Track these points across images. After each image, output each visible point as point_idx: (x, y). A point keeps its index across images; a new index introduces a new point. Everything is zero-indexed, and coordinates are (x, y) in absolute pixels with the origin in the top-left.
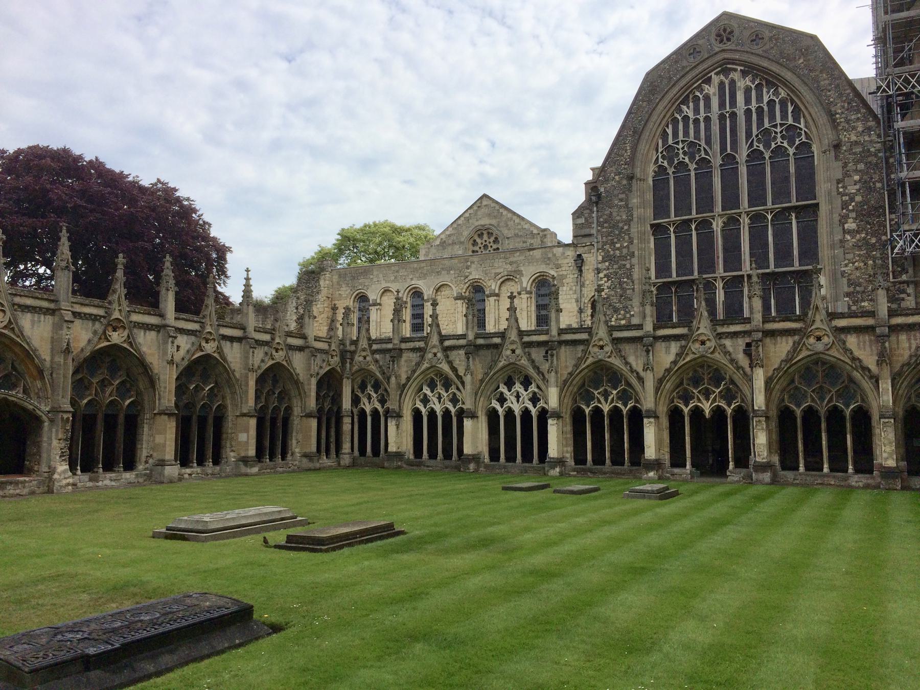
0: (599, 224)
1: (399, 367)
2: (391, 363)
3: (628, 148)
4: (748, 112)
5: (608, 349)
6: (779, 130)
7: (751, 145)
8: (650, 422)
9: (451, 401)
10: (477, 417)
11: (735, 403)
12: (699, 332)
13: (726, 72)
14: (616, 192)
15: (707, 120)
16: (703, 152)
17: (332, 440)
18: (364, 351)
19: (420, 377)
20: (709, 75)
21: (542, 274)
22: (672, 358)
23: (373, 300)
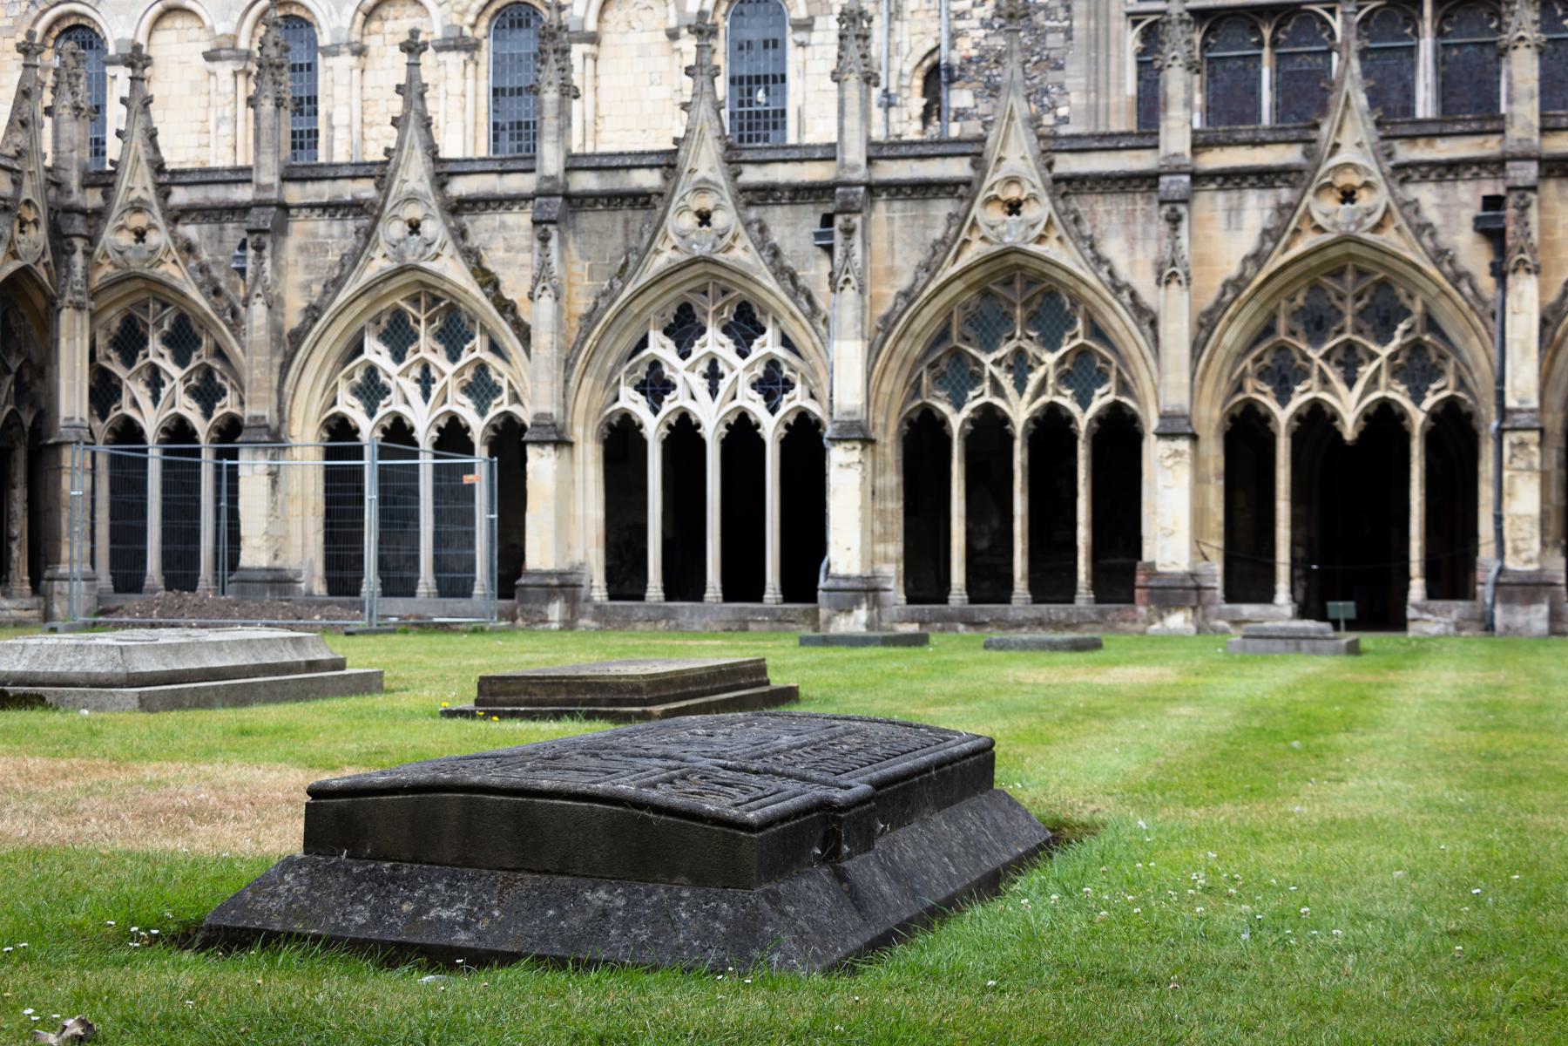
2: (251, 253)
5: (1037, 212)
8: (1177, 453)
9: (468, 390)
10: (571, 444)
11: (1437, 391)
12: (1338, 159)
17: (15, 532)
18: (138, 210)
19: (362, 303)
22: (1247, 242)
23: (119, 42)
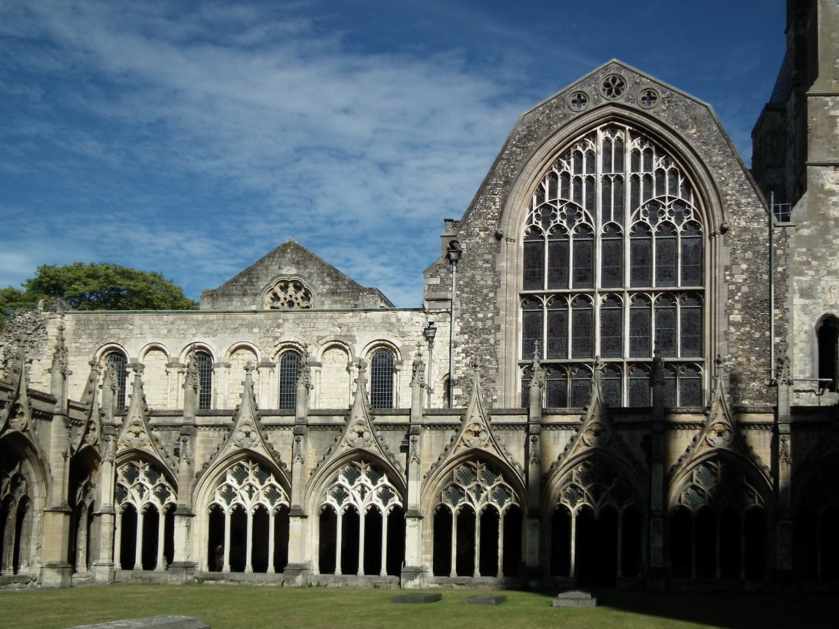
0: (459, 288)
1: (193, 449)
3: (497, 200)
4: (635, 178)
6: (667, 204)
7: (638, 216)
9: (268, 495)
13: (613, 129)
14: (479, 251)
15: (591, 180)
16: (583, 217)
20: (594, 130)
21: (382, 342)
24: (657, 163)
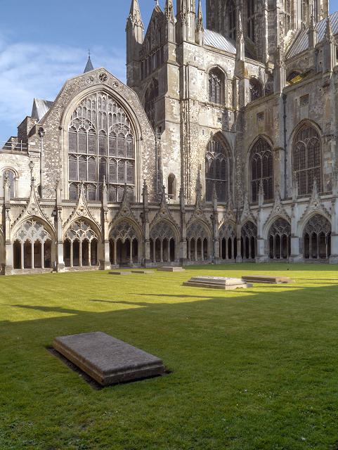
24: (118, 110)
